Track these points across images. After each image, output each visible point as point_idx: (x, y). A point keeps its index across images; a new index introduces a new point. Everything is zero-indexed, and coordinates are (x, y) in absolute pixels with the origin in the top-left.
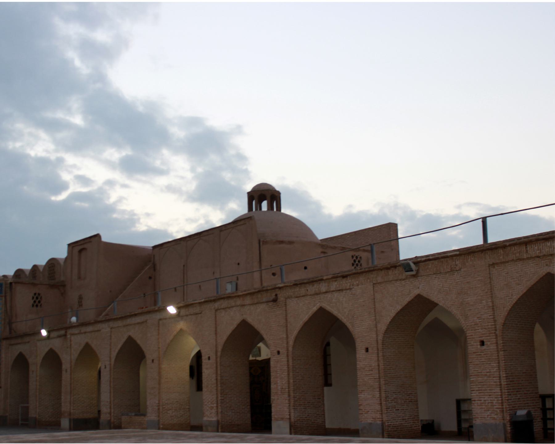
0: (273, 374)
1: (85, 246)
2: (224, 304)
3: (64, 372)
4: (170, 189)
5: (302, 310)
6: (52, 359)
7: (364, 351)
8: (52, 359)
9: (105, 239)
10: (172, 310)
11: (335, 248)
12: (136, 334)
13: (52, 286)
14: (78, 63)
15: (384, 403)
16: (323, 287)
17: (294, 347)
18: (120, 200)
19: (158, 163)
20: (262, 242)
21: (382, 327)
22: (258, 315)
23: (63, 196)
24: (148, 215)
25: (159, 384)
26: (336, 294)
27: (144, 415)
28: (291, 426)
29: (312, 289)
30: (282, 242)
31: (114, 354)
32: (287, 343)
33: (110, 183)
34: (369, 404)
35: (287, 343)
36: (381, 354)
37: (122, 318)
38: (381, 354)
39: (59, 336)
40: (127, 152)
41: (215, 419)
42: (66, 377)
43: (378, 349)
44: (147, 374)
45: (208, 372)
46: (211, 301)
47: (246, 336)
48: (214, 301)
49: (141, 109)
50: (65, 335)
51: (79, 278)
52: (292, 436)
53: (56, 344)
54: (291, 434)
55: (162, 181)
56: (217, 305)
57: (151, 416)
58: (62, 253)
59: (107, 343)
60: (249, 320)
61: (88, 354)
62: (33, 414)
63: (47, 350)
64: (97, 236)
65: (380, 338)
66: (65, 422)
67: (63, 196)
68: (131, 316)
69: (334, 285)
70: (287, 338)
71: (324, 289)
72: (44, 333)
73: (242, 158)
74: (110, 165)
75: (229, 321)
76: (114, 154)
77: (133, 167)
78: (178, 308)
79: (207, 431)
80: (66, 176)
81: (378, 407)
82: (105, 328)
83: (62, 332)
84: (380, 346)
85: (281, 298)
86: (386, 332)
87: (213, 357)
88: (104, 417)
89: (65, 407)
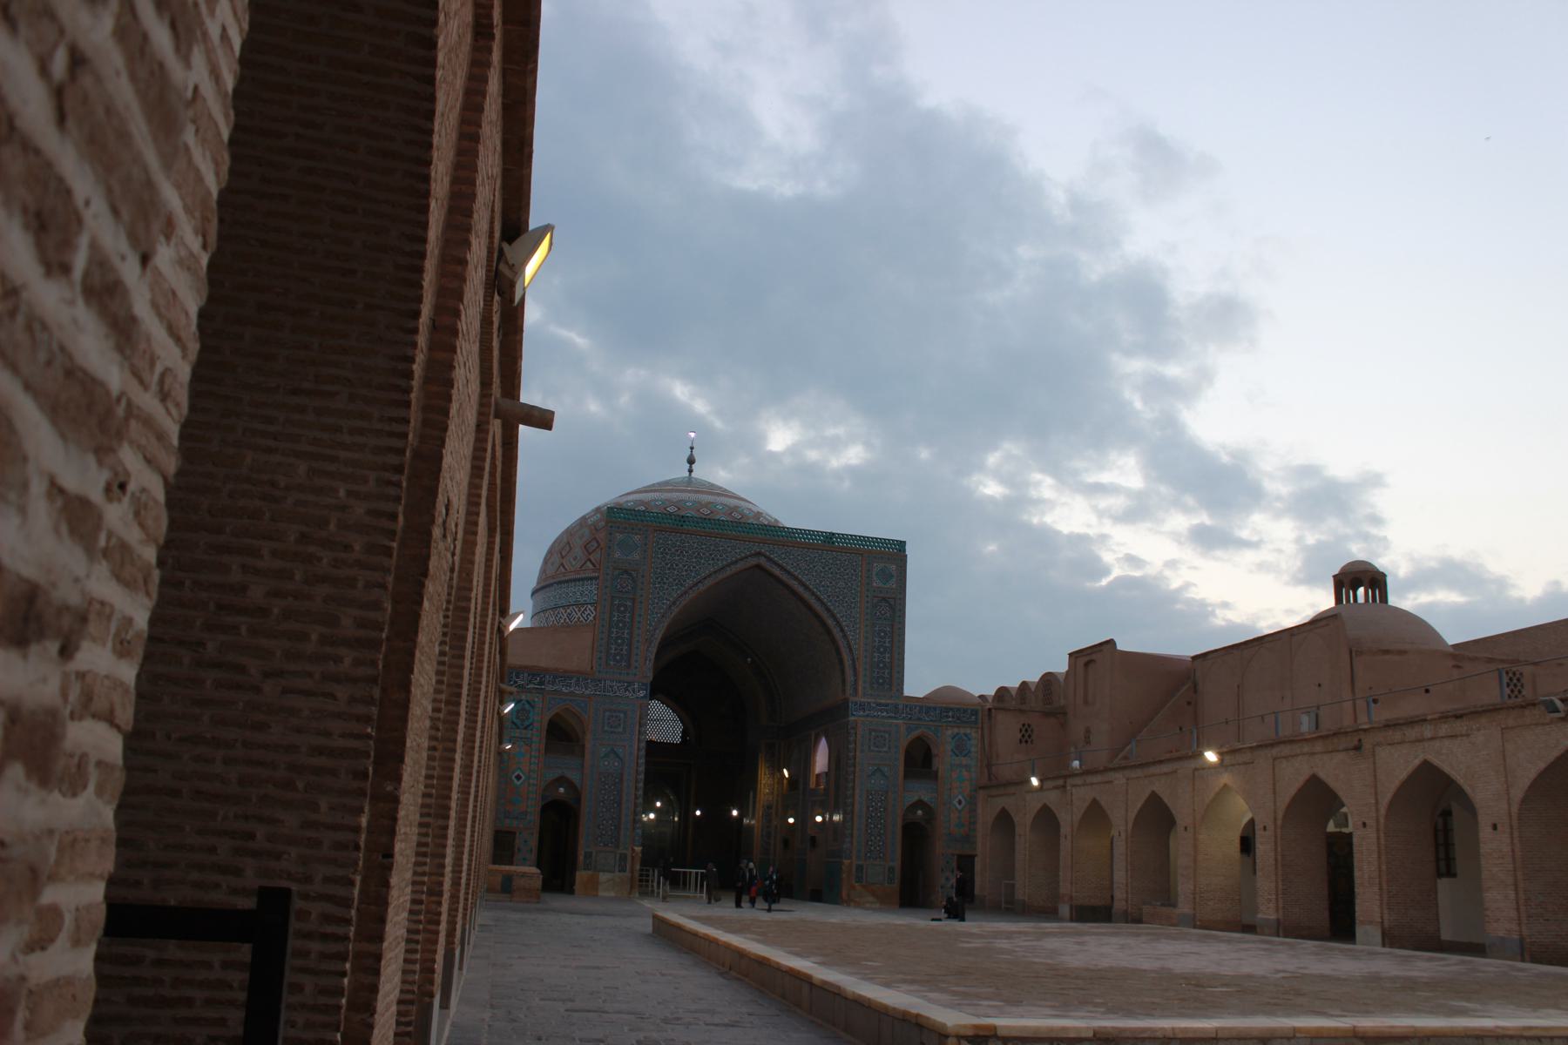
0: (1356, 856)
1: (1093, 657)
2: (1286, 750)
3: (1062, 840)
4: (1262, 567)
5: (1398, 763)
6: (1047, 819)
7: (1490, 829)
8: (1047, 819)
9: (1121, 646)
10: (1211, 756)
11: (1474, 659)
12: (1160, 787)
13: (1047, 714)
14: (1138, 404)
15: (1522, 908)
16: (1428, 731)
17: (1387, 817)
18: (1187, 586)
19: (1244, 534)
20: (1355, 651)
21: (1518, 793)
22: (1332, 768)
23: (1104, 582)
24: (1225, 605)
25: (1195, 861)
26: (1447, 742)
27: (1174, 906)
28: (1384, 934)
29: (1412, 733)
30: (1387, 652)
31: (1132, 815)
32: (1377, 810)
33: (1172, 564)
34: (1501, 910)
35: (1377, 810)
36: (1516, 834)
37: (1141, 766)
38: (1516, 834)
39: (1056, 788)
40: (1204, 518)
41: (1273, 917)
42: (1065, 845)
43: (1511, 827)
44: (1180, 845)
45: (1263, 847)
46: (1266, 746)
47: (1317, 799)
48: (1272, 745)
49: (1225, 459)
50: (1064, 787)
51: (1086, 702)
52: (1387, 950)
53: (1052, 798)
54: (1384, 945)
55: (1249, 556)
56: (1275, 751)
57: (1184, 908)
58: (1061, 666)
59: (1123, 799)
60: (1322, 775)
61: (1096, 815)
62: (1020, 895)
63: (1039, 806)
64: (1111, 643)
65: (1515, 809)
66: (1065, 910)
67: (1104, 582)
68: (1154, 763)
69: (1444, 729)
70: (1377, 802)
71: (1428, 734)
72: (1035, 781)
73: (1376, 520)
74: (1176, 537)
75: (1294, 773)
76: (1180, 522)
77: (1208, 540)
78: (1221, 754)
79: (1263, 934)
80: (1107, 557)
81: (1513, 914)
82: (1119, 778)
83: (1060, 782)
84: (1515, 823)
85: (1367, 745)
86: (1524, 801)
87: (1271, 827)
88: (1119, 905)
89: (1065, 888)
